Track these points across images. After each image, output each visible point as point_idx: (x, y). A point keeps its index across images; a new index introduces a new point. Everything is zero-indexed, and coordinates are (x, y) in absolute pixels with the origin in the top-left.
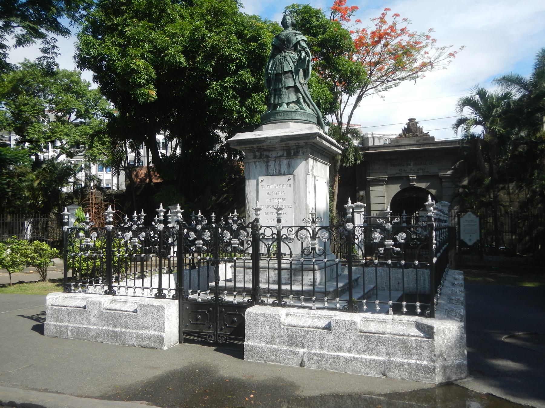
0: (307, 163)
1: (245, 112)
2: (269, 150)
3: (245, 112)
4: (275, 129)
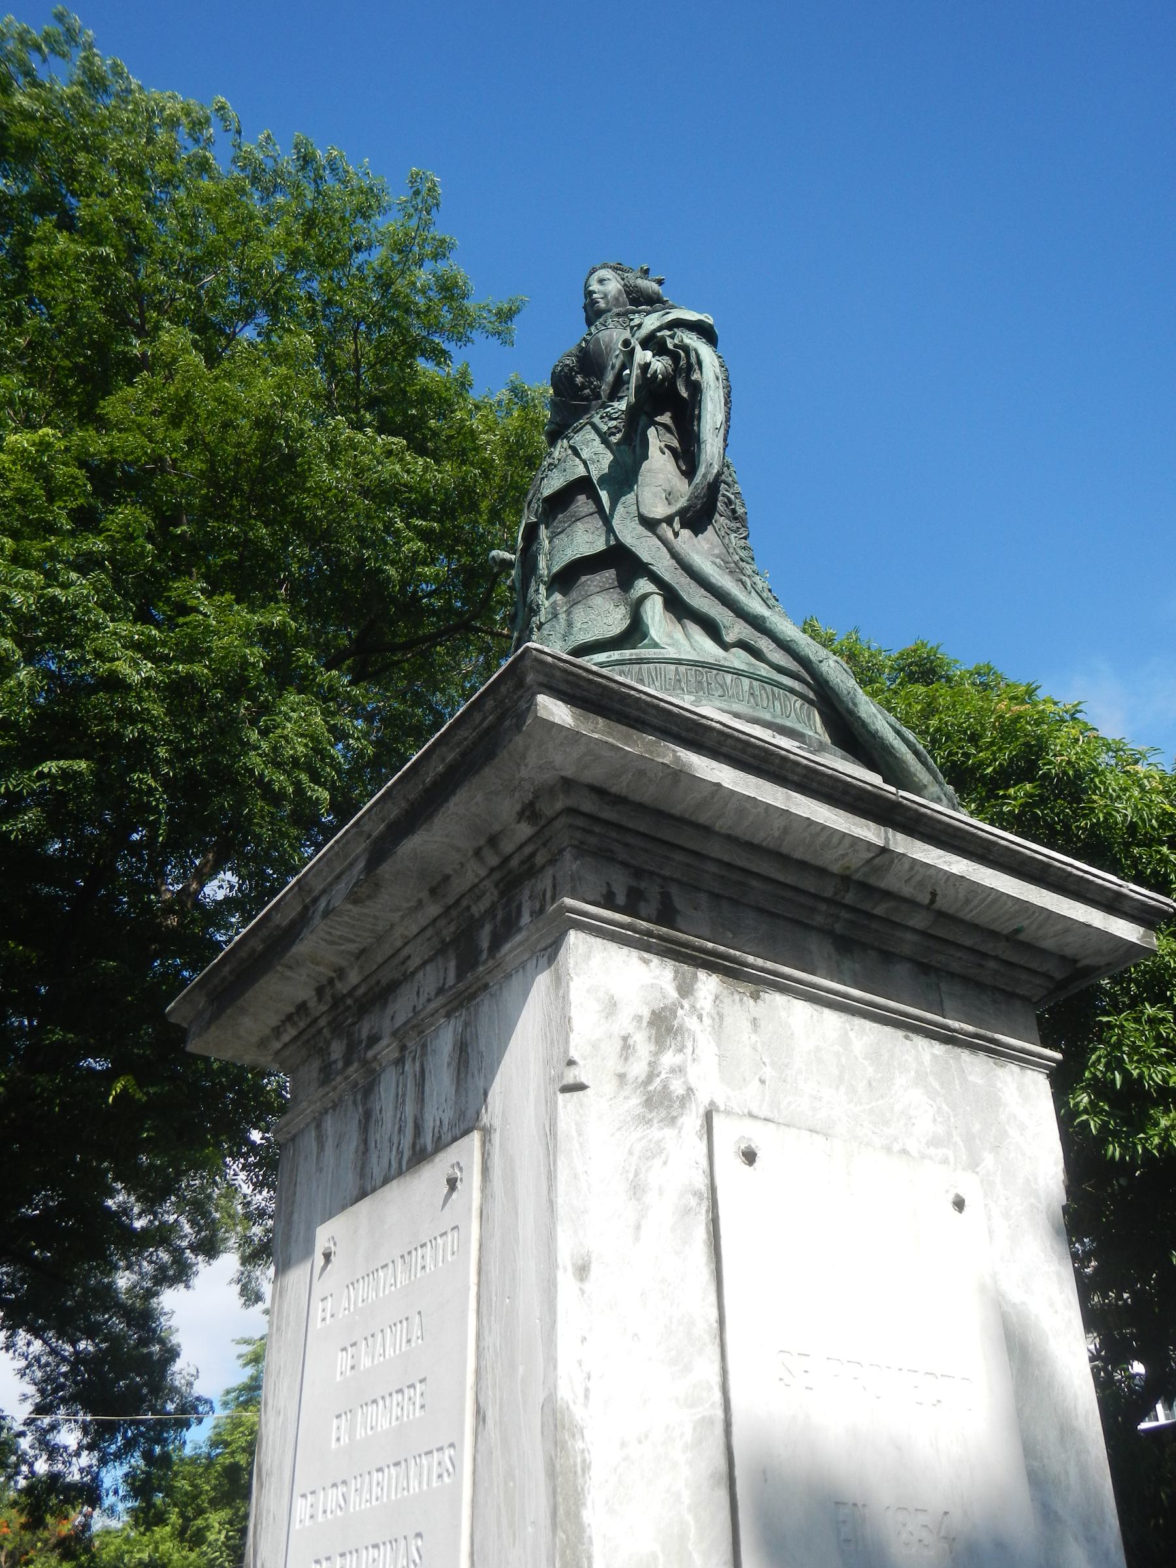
0: (559, 982)
1: (1093, 1109)
2: (380, 995)
3: (1093, 1109)
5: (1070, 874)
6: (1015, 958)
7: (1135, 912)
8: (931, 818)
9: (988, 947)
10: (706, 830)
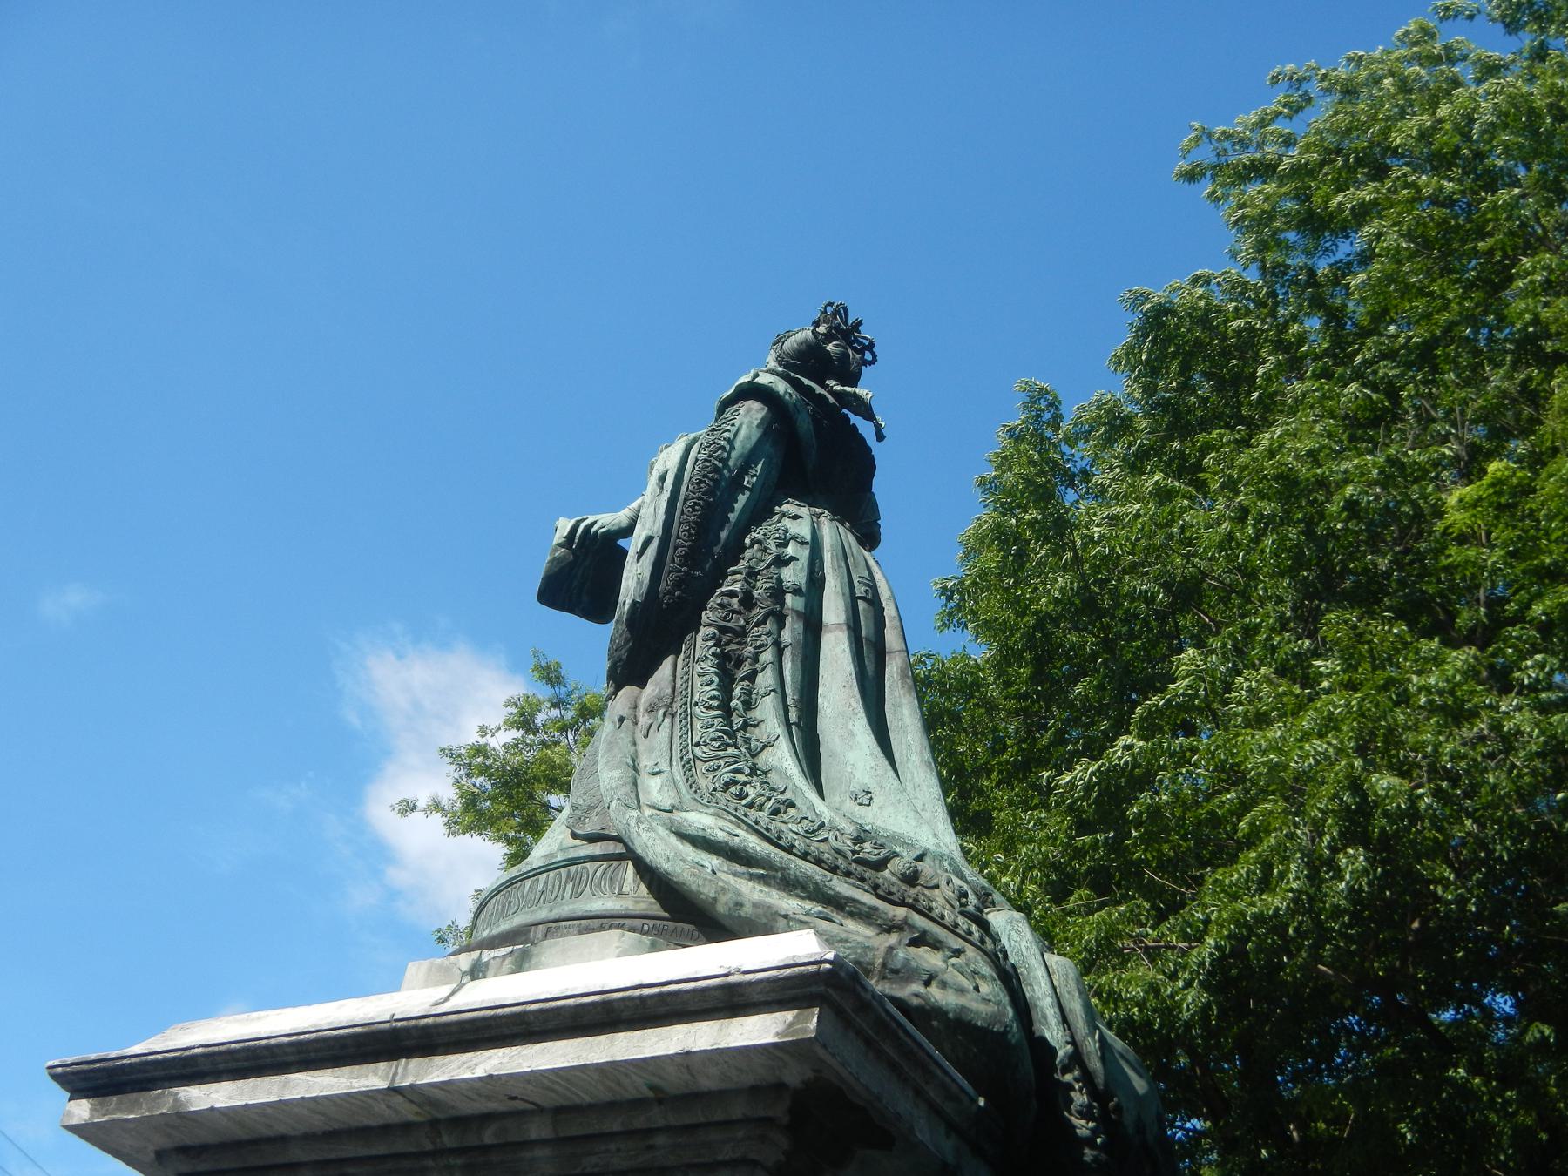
5: (642, 998)
6: (687, 1119)
7: (774, 996)
8: (436, 1026)
9: (639, 1122)
10: (282, 1140)
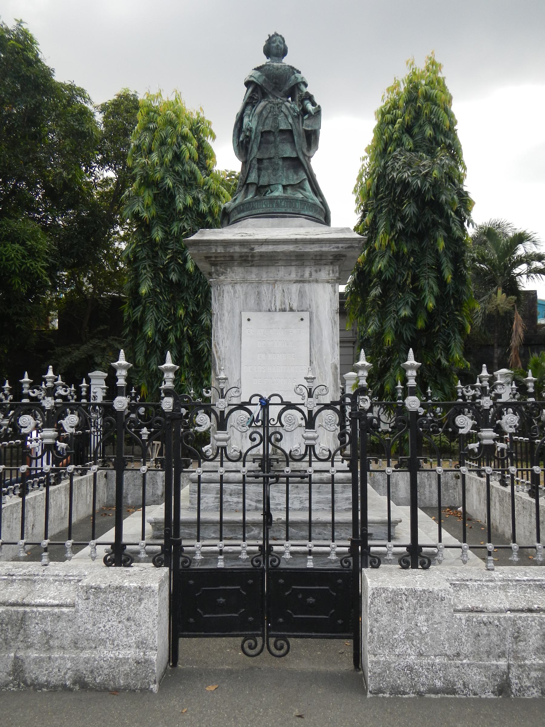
4: (273, 226)
